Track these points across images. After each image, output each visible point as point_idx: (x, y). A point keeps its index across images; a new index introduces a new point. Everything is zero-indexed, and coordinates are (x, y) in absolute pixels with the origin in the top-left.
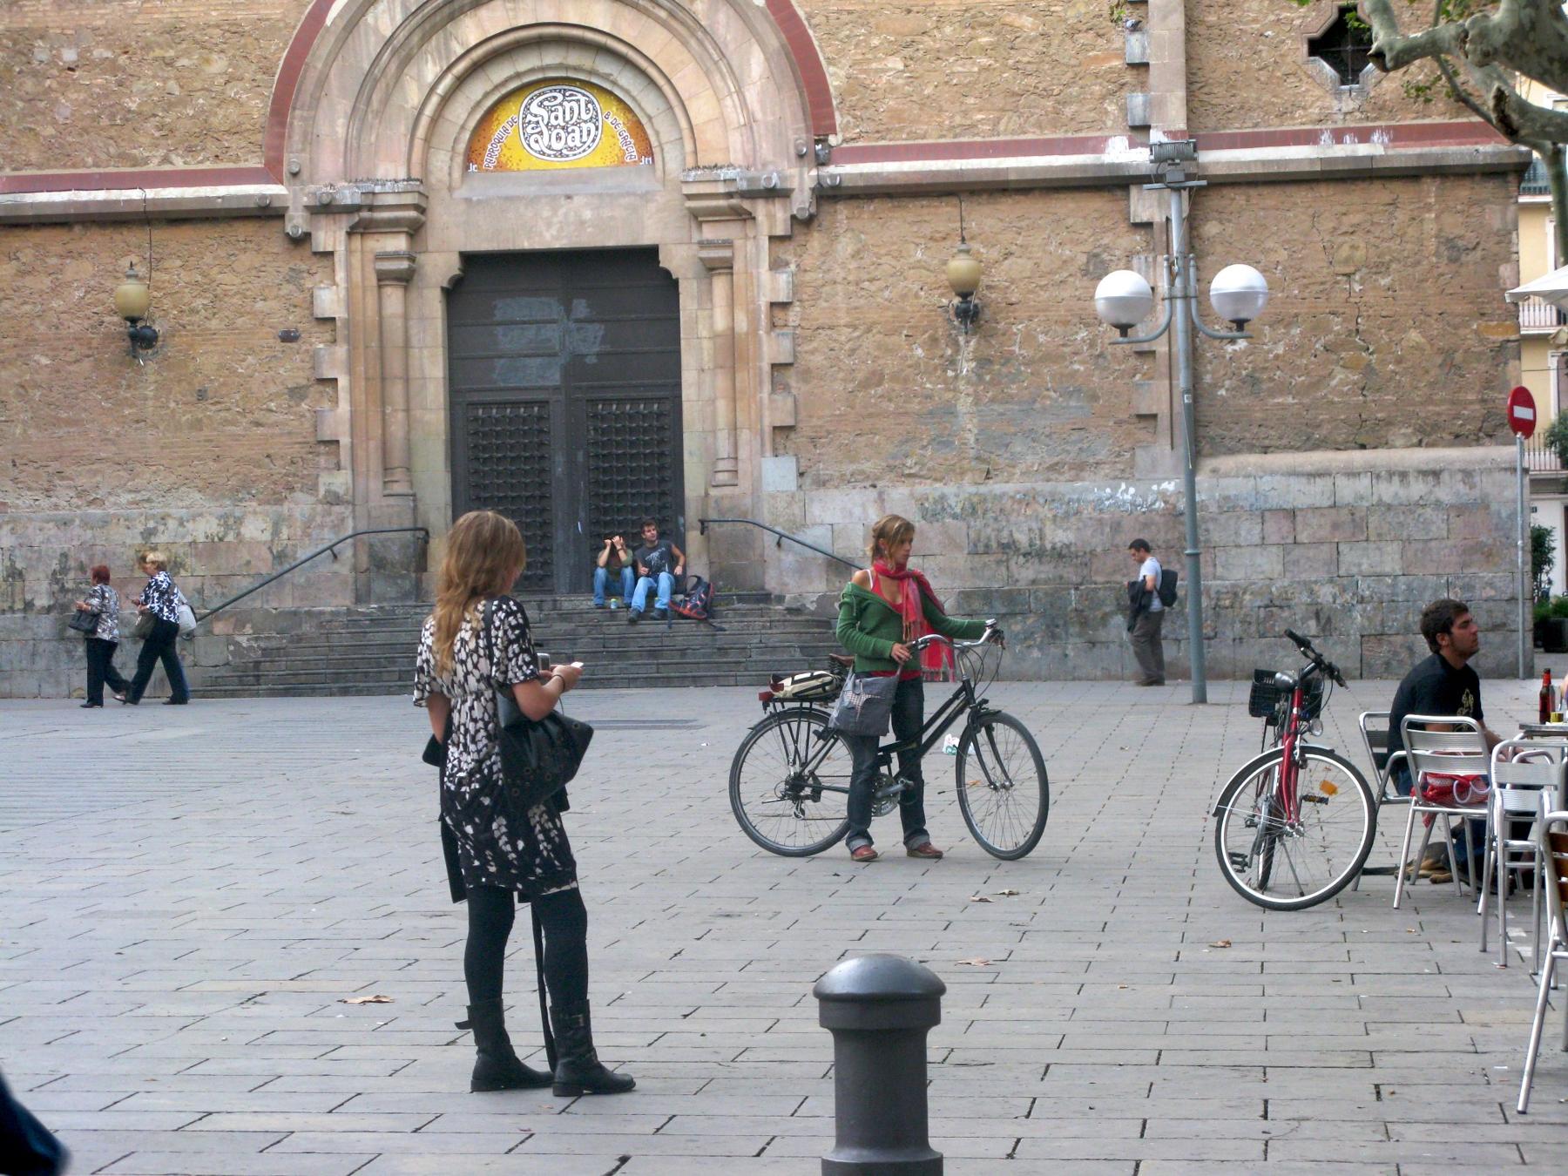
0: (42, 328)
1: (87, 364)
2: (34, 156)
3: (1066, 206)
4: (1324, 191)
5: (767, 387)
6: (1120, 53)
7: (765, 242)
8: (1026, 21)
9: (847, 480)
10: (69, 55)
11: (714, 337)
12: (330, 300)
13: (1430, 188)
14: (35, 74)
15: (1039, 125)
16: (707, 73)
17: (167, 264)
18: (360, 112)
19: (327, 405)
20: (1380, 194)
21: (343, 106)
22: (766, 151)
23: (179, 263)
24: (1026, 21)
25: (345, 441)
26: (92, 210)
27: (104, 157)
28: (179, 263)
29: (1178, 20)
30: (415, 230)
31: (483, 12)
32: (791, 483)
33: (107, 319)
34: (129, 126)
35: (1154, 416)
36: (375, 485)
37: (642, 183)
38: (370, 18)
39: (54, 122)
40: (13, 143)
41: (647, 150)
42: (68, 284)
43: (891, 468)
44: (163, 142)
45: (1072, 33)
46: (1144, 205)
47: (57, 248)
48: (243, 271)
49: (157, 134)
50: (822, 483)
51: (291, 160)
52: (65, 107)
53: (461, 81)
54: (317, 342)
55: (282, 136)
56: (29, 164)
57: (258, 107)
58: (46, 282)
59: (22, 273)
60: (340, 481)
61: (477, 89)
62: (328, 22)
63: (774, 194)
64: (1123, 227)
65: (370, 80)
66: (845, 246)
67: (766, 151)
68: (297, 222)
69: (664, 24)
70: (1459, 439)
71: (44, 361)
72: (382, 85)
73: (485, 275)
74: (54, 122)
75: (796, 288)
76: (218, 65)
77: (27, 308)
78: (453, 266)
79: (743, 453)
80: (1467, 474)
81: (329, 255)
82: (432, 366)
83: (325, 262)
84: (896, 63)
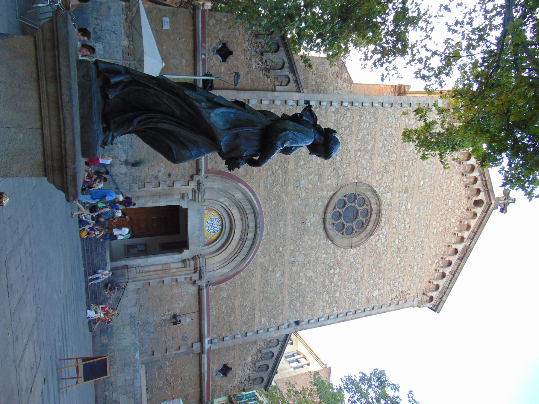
3: (197, 331)
4: (198, 373)
5: (159, 280)
8: (232, 318)
12: (178, 185)
13: (198, 390)
15: (213, 323)
16: (224, 259)
18: (219, 189)
19: (153, 184)
20: (197, 382)
21: (220, 187)
24: (232, 318)
25: (145, 189)
31: (238, 214)
35: (153, 355)
38: (239, 192)
41: (209, 244)
43: (141, 306)
46: (197, 346)
54: (169, 182)
55: (215, 174)
61: (222, 210)
62: (239, 184)
63: (200, 277)
64: (193, 342)
65: (226, 192)
67: (209, 274)
68: (196, 178)
69: (234, 250)
72: (224, 194)
75: (181, 283)
83: (186, 184)
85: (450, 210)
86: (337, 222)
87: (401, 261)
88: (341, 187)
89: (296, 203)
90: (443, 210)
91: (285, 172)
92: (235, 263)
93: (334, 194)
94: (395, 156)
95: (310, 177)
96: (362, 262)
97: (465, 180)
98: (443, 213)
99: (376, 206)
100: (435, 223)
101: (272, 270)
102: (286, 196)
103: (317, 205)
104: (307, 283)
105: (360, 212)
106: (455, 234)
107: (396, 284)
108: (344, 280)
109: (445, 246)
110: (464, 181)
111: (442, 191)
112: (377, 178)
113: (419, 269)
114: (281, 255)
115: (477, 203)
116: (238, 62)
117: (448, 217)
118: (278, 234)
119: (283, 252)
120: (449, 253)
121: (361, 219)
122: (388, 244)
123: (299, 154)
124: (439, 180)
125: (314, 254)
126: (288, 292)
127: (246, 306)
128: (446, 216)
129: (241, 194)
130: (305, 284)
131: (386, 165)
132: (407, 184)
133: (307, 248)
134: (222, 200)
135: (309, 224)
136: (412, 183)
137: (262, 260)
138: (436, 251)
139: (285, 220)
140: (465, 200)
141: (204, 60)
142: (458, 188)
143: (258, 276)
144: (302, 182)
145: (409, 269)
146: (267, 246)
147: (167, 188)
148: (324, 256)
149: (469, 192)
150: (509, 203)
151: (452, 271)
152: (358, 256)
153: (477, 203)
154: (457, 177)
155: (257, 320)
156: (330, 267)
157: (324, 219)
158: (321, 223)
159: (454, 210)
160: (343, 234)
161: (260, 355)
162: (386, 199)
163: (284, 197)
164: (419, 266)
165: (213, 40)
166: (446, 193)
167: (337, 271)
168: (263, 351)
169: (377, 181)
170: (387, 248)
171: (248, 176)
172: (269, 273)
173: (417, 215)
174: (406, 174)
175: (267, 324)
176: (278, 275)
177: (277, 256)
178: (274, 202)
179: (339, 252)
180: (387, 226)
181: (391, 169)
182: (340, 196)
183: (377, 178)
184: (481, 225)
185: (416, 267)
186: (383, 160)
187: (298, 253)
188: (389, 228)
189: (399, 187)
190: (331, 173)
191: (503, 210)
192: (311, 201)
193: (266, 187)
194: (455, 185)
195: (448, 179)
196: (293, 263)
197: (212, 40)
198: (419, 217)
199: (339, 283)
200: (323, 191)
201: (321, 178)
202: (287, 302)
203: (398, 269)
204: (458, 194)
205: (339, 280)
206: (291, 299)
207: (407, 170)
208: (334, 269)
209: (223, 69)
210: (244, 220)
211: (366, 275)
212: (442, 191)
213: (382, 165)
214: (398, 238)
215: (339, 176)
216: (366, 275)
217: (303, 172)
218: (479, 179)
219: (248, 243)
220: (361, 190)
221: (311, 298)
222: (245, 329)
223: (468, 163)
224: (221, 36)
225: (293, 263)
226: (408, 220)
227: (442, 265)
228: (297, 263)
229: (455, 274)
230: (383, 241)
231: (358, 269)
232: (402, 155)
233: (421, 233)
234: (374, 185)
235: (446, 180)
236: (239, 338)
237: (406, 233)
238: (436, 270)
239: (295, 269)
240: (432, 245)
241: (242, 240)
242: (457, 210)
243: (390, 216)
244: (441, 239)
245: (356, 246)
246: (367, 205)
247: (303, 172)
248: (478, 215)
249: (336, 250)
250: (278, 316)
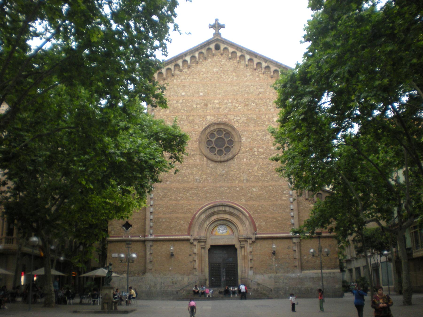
6: (291, 222)
7: (249, 244)
8: (279, 218)
9: (259, 274)
10: (164, 220)
11: (242, 256)
12: (196, 251)
18: (199, 228)
22: (249, 233)
24: (279, 218)
25: (197, 268)
29: (297, 219)
30: (205, 242)
32: (252, 274)
36: (200, 274)
37: (233, 237)
38: (201, 217)
45: (285, 220)
46: (294, 240)
48: (185, 246)
50: (256, 274)
51: (192, 233)
53: (211, 224)
57: (187, 227)
60: (196, 273)
61: (213, 225)
63: (250, 238)
65: (201, 224)
66: (259, 245)
70: (332, 269)
73: (214, 248)
75: (253, 250)
76: (182, 222)
78: (209, 247)
79: (246, 270)
80: (334, 273)
81: (195, 245)
82: (207, 259)
84: (264, 223)
85: (221, 69)
86: (224, 152)
87: (254, 102)
88: (201, 152)
89: (210, 181)
90: (221, 74)
91: (191, 188)
92: (243, 218)
93: (206, 156)
94: (184, 116)
95: (195, 173)
96: (252, 132)
97: (201, 60)
98: (223, 74)
99: (215, 126)
100: (229, 80)
101: (251, 194)
102: (205, 187)
103: (212, 167)
104: (262, 170)
105: (218, 136)
106: (238, 62)
107: (271, 104)
108: (263, 144)
109: (247, 69)
110: (202, 61)
111: (208, 77)
112: (197, 127)
113: (262, 86)
114: (242, 189)
115: (217, 48)
117: (226, 69)
118: (228, 191)
119: (240, 187)
120: (252, 64)
121: (223, 135)
122: (241, 114)
123: (181, 181)
124: (200, 81)
125: (243, 167)
126: (267, 182)
127: (273, 210)
128: (225, 71)
129: (202, 215)
130: (263, 172)
131: (189, 122)
132: (202, 105)
133: (238, 172)
134: (205, 226)
135: (224, 172)
136: (201, 101)
137: (244, 201)
138: (250, 76)
139: (220, 187)
140: (215, 58)
141: (132, 236)
142: (207, 65)
143: (254, 202)
144: (197, 177)
145: (261, 95)
146: (235, 198)
147: (197, 257)
148: (245, 160)
149: (209, 55)
150: (218, 24)
151: (264, 61)
152: (247, 135)
153: (217, 48)
154: (199, 67)
155: (283, 202)
156: (253, 155)
157: (221, 162)
158: (223, 164)
159: (222, 65)
160: (232, 147)
161: (309, 199)
162: (210, 119)
163: (205, 189)
164: (259, 87)
166: (209, 74)
167: (256, 149)
168: (307, 197)
169: (199, 127)
170: (244, 114)
171: (192, 211)
172: (253, 196)
173: (223, 94)
174: (195, 106)
175: (287, 195)
176: (254, 190)
177: (242, 191)
178: (208, 195)
179: (243, 150)
180: (229, 116)
181: (191, 118)
182: (207, 152)
183: (197, 127)
184: (232, 45)
185: (260, 90)
186: (186, 125)
187: (242, 178)
188: (230, 115)
189: (203, 111)
190: (192, 160)
191: (223, 26)
192: (209, 171)
193: (199, 200)
194: (204, 68)
195: (200, 74)
196: (247, 181)
198: (224, 93)
199: (265, 147)
200: (203, 163)
201: (196, 166)
202: (274, 183)
203: (260, 104)
204: (210, 64)
205: (263, 148)
206: (272, 180)
207: (192, 106)
208: (255, 152)
209: (135, 226)
210: (218, 213)
211: (262, 128)
212: (208, 77)
213: (189, 125)
214: (237, 107)
215: (194, 154)
216: (262, 128)
217: (191, 177)
218: (200, 51)
219: (232, 210)
220: (204, 137)
221: (273, 167)
222: (288, 210)
223: (189, 62)
225: (247, 181)
226: (226, 101)
227: (260, 69)
228: (248, 178)
229: (266, 60)
230: (238, 118)
231: (257, 135)
232: (183, 111)
233: (236, 90)
234: (201, 129)
235: (201, 75)
236: (294, 214)
237: (235, 101)
238: (264, 73)
239: (251, 179)
240: (245, 79)
241: (231, 214)
242: (222, 63)
243: (222, 115)
244: (241, 73)
245: (241, 138)
246: (215, 131)
247: (191, 177)
248: (226, 46)
249: (242, 152)
250: (283, 188)
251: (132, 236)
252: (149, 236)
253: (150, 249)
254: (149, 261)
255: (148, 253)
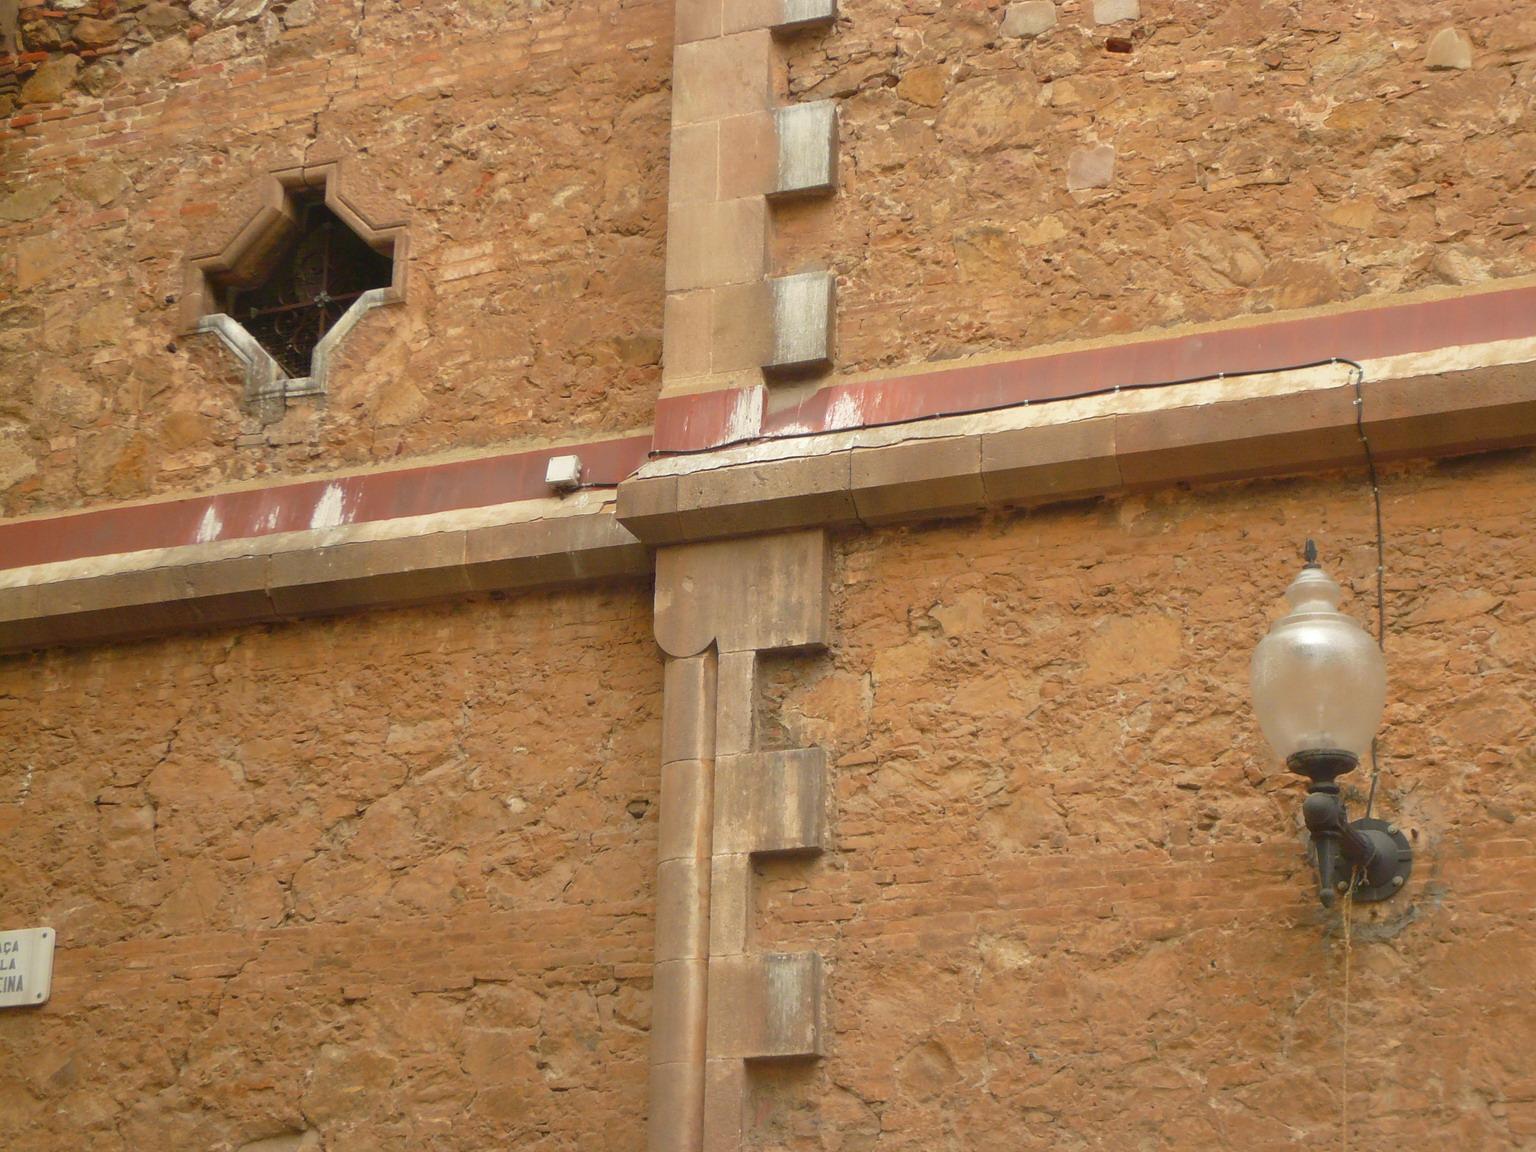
0: (1008, 848)
1: (1154, 969)
2: (996, 312)
14: (1008, 72)
17: (1441, 604)
23: (1482, 598)
26: (1178, 438)
27: (1219, 286)
28: (1482, 598)
33: (1229, 805)
34: (1304, 184)
39: (1064, 201)
40: (935, 281)
42: (1097, 697)
44: (1416, 217)
47: (1064, 583)
49: (1397, 196)
52: (1095, 163)
56: (981, 336)
58: (1024, 693)
59: (948, 672)
71: (1012, 957)
74: (1064, 201)
77: (961, 780)
116: (399, 104)
141: (369, 500)
165: (172, 425)
197: (175, 434)
209: (466, 263)
224: (145, 341)
251: (369, 500)
252: (747, 417)
253: (768, 727)
254: (726, 1064)
255: (715, 849)
